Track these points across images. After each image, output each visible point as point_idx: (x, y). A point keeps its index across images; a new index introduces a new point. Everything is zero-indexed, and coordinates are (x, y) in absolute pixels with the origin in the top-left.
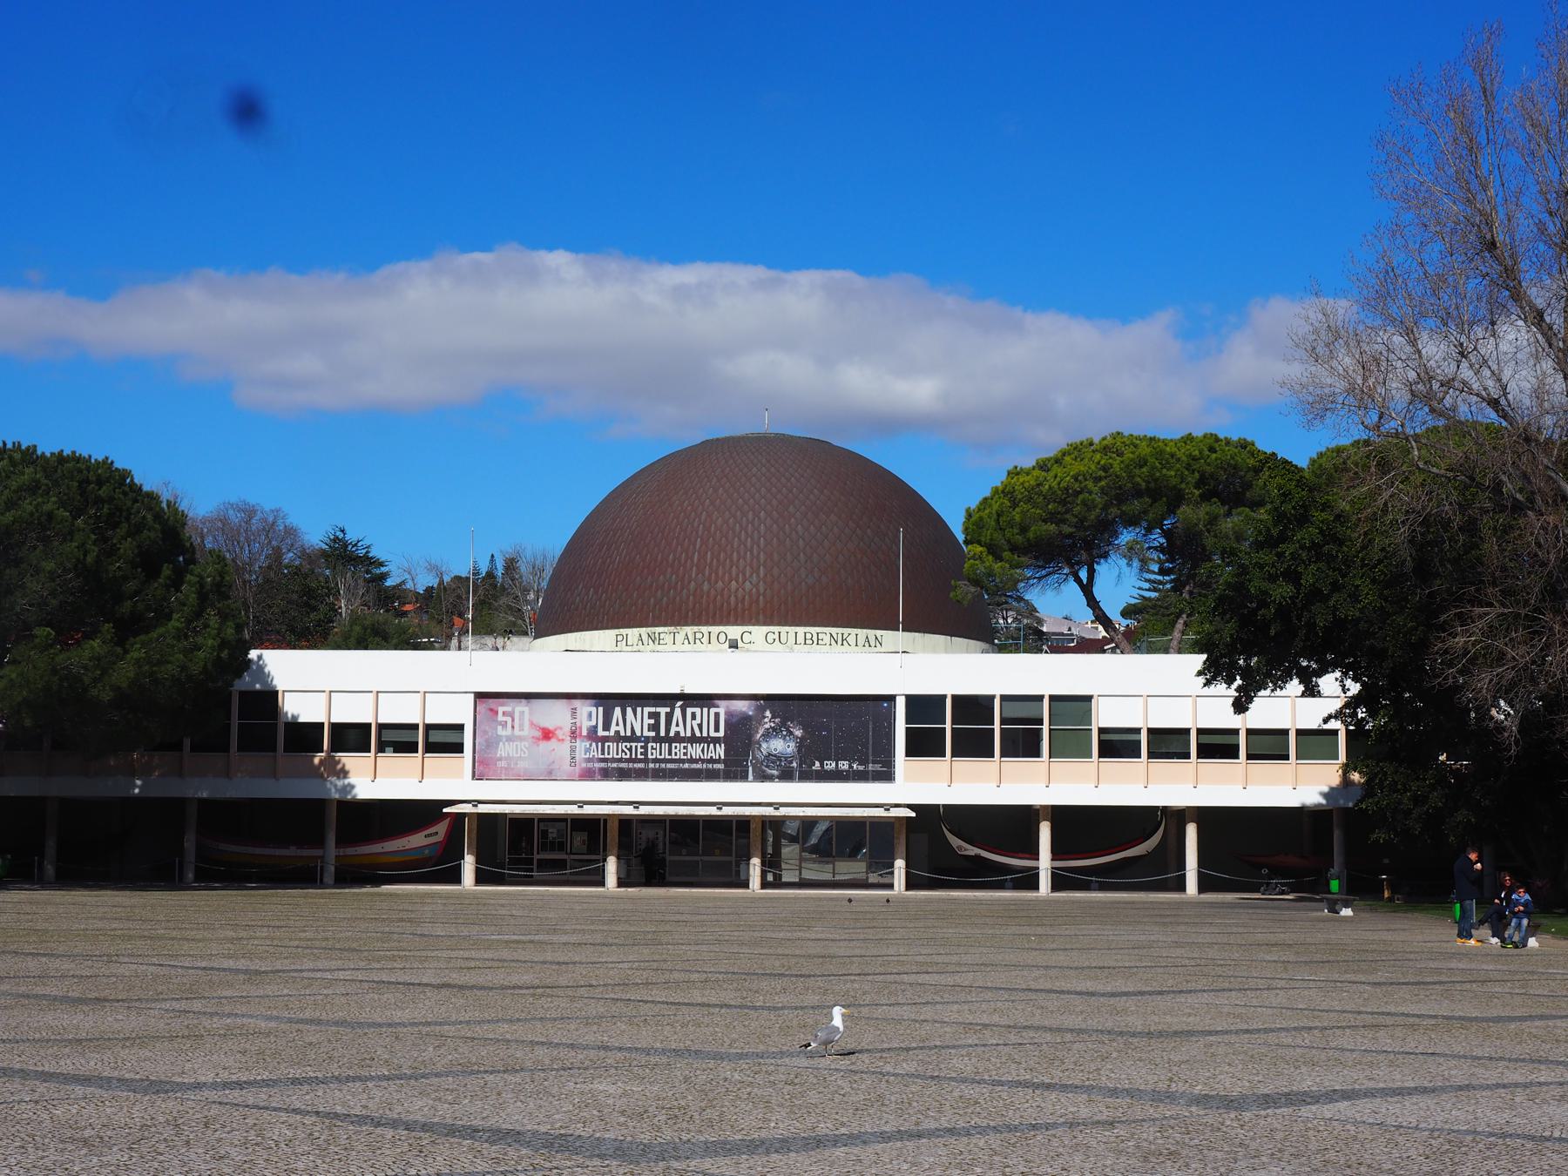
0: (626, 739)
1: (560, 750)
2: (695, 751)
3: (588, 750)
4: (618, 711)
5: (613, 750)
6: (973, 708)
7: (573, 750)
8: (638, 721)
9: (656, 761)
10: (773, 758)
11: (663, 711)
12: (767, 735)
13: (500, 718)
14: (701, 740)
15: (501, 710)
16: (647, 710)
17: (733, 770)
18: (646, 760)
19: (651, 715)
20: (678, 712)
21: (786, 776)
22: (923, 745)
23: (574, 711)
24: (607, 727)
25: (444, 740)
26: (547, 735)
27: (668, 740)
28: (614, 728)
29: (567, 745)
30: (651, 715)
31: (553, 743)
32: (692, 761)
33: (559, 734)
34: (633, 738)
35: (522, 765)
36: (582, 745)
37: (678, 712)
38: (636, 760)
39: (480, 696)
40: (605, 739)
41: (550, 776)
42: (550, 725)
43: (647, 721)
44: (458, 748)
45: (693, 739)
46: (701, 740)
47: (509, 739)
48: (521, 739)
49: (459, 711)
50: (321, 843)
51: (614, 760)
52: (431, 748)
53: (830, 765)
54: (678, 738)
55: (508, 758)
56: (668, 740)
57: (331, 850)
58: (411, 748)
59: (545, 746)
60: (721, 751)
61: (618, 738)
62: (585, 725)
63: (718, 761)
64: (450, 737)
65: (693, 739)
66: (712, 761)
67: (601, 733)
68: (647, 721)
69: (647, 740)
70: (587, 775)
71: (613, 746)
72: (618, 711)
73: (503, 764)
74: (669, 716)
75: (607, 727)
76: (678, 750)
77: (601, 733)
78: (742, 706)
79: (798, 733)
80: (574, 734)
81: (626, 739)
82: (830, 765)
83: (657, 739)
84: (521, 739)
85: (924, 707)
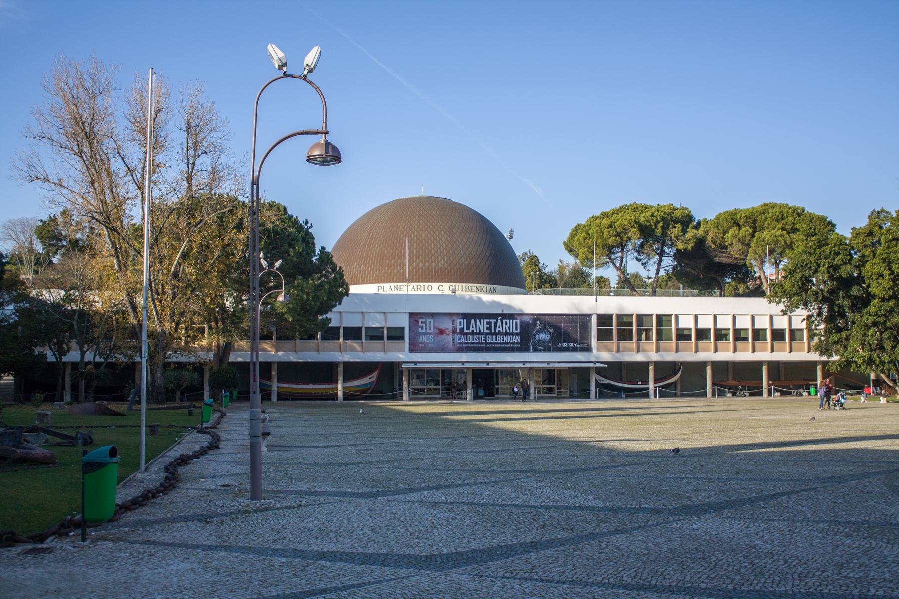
0: (477, 334)
1: (448, 339)
2: (507, 339)
3: (460, 339)
4: (473, 321)
5: (471, 339)
6: (624, 320)
7: (453, 339)
8: (482, 326)
9: (490, 343)
10: (541, 342)
11: (493, 321)
12: (538, 332)
13: (420, 324)
14: (510, 334)
15: (420, 321)
16: (486, 321)
17: (523, 347)
18: (486, 343)
19: (488, 323)
20: (499, 321)
21: (547, 349)
22: (604, 335)
23: (453, 322)
24: (468, 328)
25: (396, 335)
26: (441, 332)
27: (496, 334)
28: (471, 329)
29: (451, 337)
30: (488, 323)
31: (444, 336)
32: (506, 343)
33: (447, 331)
34: (480, 333)
35: (430, 345)
36: (457, 337)
37: (499, 321)
38: (482, 343)
39: (411, 315)
40: (467, 334)
41: (443, 350)
42: (442, 327)
43: (486, 326)
44: (402, 338)
45: (506, 334)
46: (510, 334)
47: (425, 334)
48: (430, 334)
49: (403, 322)
50: (336, 382)
51: (472, 343)
52: (390, 338)
53: (565, 345)
54: (499, 333)
55: (424, 343)
56: (496, 334)
57: (340, 386)
58: (381, 338)
59: (440, 336)
60: (518, 339)
61: (473, 333)
62: (459, 327)
63: (518, 343)
64: (398, 334)
65: (506, 334)
66: (514, 343)
67: (465, 331)
68: (486, 326)
69: (487, 334)
70: (460, 350)
71: (471, 337)
72: (473, 321)
73: (421, 345)
74: (496, 323)
75: (468, 328)
76: (500, 339)
77: (465, 331)
78: (527, 319)
79: (551, 331)
80: (454, 331)
81: (477, 334)
82: (565, 345)
83: (491, 334)
84: (430, 334)
85: (605, 320)
